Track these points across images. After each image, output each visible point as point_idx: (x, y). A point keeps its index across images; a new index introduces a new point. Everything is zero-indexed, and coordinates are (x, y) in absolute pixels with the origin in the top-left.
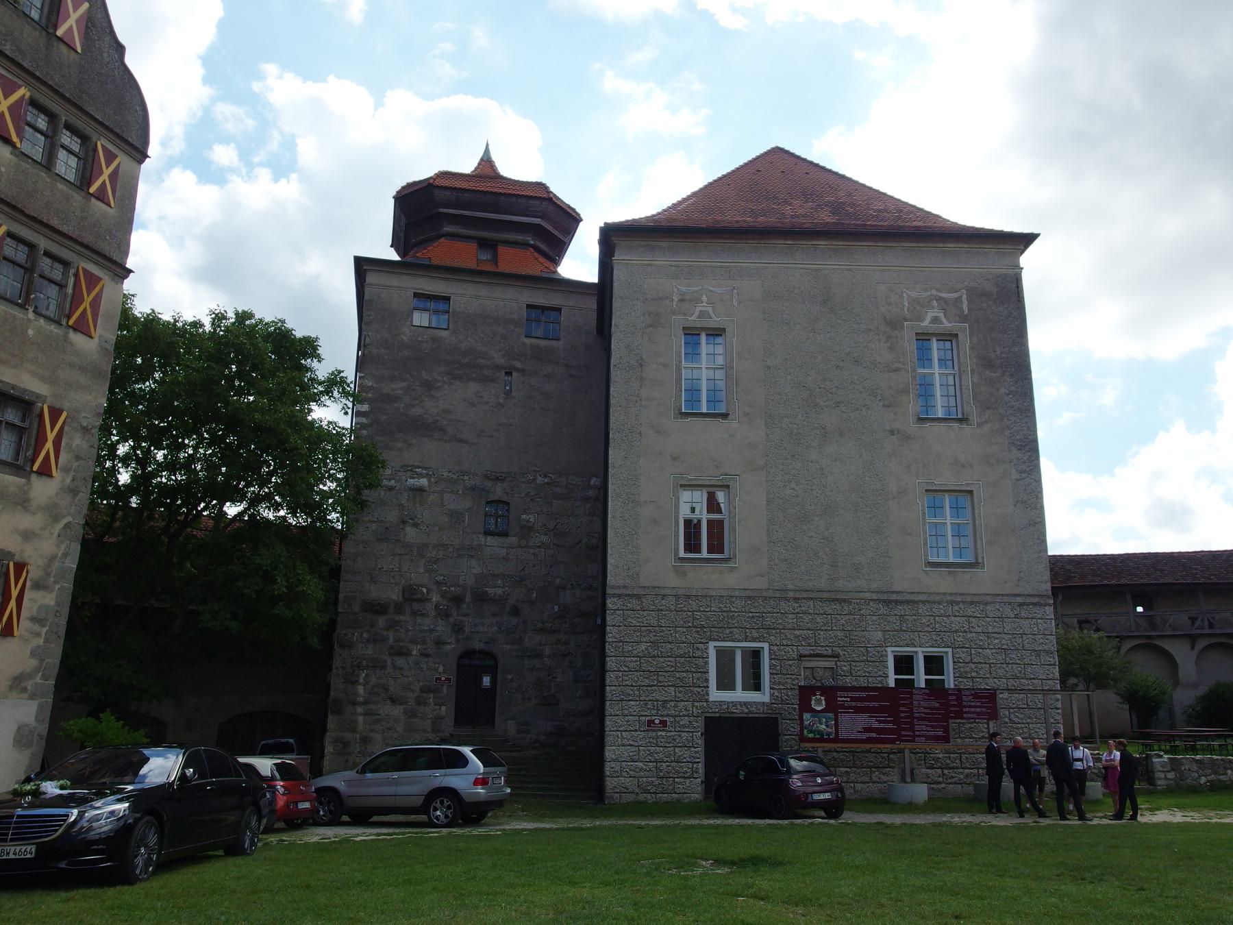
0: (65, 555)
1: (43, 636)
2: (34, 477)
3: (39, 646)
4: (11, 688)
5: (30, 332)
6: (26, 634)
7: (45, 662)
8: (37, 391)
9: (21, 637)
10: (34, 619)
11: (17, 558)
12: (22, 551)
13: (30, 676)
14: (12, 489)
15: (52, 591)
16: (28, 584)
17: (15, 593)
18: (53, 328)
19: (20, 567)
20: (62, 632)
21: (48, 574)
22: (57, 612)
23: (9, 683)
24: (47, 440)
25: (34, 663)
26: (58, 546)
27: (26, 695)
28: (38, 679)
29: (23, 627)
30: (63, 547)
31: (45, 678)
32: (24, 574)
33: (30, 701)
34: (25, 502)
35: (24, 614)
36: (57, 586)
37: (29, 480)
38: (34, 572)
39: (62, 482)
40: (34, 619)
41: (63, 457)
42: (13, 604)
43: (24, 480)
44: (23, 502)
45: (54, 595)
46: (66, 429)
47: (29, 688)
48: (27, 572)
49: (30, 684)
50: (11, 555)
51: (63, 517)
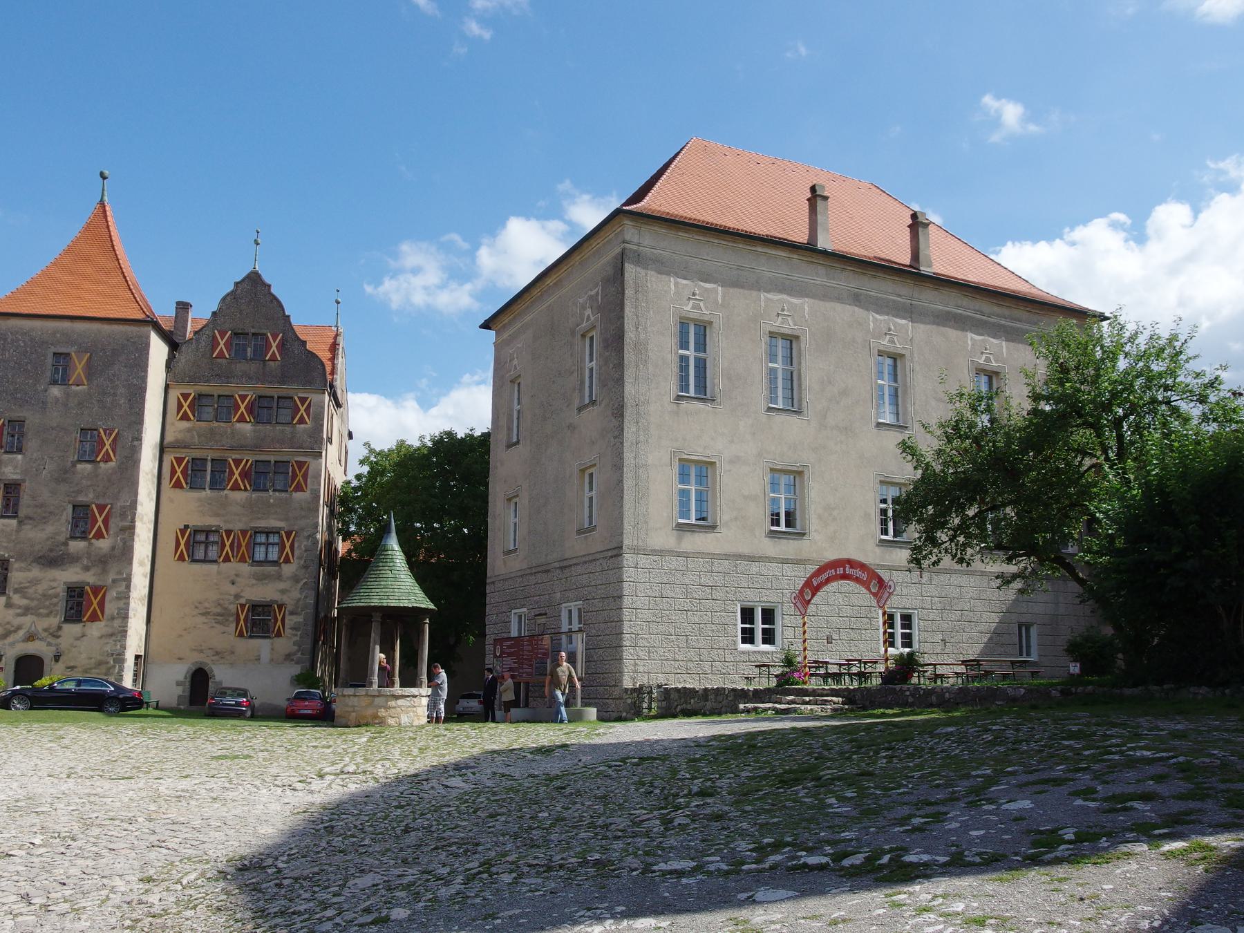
0: (306, 597)
2: (283, 565)
4: (285, 659)
5: (272, 501)
10: (291, 629)
11: (279, 603)
14: (273, 573)
16: (287, 612)
17: (279, 618)
18: (283, 495)
19: (280, 607)
25: (296, 648)
26: (301, 594)
28: (299, 655)
29: (288, 631)
30: (304, 594)
31: (302, 654)
35: (287, 626)
38: (289, 608)
41: (297, 553)
42: (279, 623)
43: (277, 568)
44: (279, 577)
45: (302, 616)
46: (296, 539)
50: (276, 602)
51: (302, 580)
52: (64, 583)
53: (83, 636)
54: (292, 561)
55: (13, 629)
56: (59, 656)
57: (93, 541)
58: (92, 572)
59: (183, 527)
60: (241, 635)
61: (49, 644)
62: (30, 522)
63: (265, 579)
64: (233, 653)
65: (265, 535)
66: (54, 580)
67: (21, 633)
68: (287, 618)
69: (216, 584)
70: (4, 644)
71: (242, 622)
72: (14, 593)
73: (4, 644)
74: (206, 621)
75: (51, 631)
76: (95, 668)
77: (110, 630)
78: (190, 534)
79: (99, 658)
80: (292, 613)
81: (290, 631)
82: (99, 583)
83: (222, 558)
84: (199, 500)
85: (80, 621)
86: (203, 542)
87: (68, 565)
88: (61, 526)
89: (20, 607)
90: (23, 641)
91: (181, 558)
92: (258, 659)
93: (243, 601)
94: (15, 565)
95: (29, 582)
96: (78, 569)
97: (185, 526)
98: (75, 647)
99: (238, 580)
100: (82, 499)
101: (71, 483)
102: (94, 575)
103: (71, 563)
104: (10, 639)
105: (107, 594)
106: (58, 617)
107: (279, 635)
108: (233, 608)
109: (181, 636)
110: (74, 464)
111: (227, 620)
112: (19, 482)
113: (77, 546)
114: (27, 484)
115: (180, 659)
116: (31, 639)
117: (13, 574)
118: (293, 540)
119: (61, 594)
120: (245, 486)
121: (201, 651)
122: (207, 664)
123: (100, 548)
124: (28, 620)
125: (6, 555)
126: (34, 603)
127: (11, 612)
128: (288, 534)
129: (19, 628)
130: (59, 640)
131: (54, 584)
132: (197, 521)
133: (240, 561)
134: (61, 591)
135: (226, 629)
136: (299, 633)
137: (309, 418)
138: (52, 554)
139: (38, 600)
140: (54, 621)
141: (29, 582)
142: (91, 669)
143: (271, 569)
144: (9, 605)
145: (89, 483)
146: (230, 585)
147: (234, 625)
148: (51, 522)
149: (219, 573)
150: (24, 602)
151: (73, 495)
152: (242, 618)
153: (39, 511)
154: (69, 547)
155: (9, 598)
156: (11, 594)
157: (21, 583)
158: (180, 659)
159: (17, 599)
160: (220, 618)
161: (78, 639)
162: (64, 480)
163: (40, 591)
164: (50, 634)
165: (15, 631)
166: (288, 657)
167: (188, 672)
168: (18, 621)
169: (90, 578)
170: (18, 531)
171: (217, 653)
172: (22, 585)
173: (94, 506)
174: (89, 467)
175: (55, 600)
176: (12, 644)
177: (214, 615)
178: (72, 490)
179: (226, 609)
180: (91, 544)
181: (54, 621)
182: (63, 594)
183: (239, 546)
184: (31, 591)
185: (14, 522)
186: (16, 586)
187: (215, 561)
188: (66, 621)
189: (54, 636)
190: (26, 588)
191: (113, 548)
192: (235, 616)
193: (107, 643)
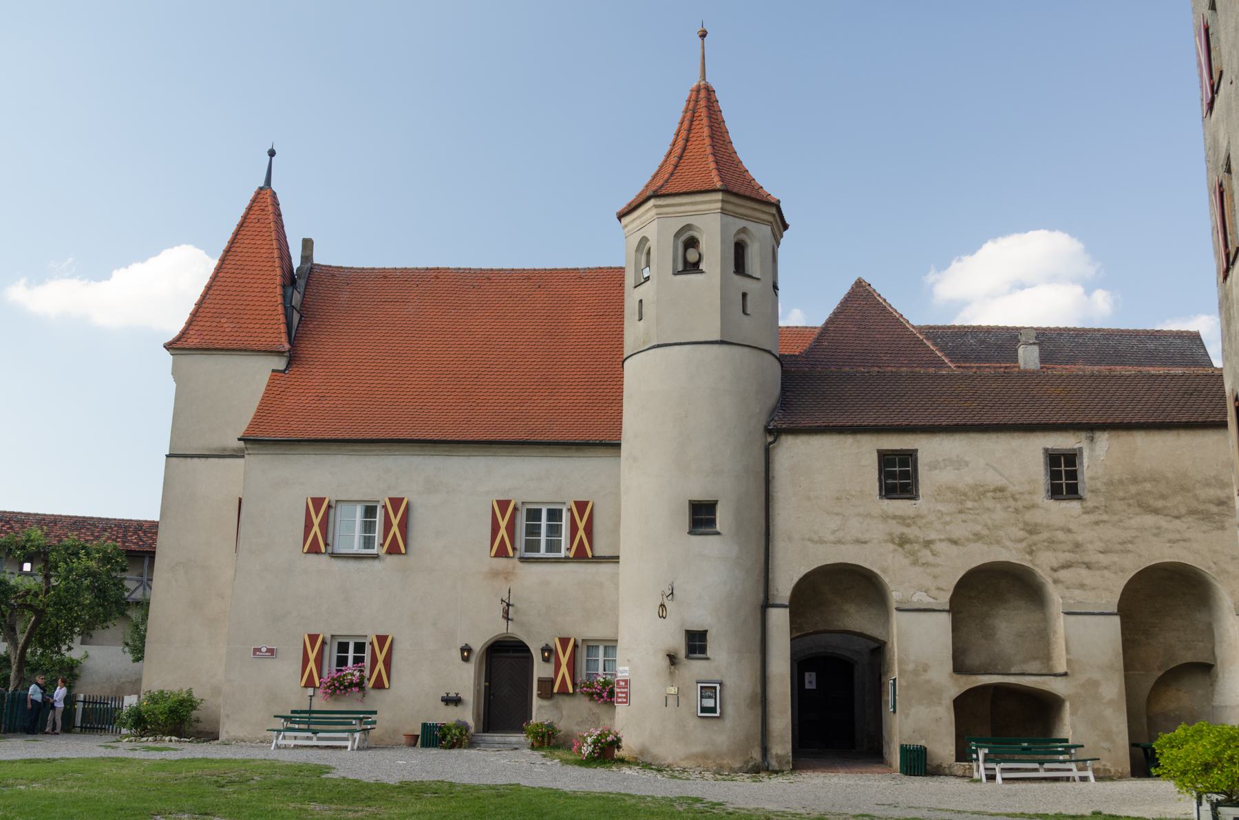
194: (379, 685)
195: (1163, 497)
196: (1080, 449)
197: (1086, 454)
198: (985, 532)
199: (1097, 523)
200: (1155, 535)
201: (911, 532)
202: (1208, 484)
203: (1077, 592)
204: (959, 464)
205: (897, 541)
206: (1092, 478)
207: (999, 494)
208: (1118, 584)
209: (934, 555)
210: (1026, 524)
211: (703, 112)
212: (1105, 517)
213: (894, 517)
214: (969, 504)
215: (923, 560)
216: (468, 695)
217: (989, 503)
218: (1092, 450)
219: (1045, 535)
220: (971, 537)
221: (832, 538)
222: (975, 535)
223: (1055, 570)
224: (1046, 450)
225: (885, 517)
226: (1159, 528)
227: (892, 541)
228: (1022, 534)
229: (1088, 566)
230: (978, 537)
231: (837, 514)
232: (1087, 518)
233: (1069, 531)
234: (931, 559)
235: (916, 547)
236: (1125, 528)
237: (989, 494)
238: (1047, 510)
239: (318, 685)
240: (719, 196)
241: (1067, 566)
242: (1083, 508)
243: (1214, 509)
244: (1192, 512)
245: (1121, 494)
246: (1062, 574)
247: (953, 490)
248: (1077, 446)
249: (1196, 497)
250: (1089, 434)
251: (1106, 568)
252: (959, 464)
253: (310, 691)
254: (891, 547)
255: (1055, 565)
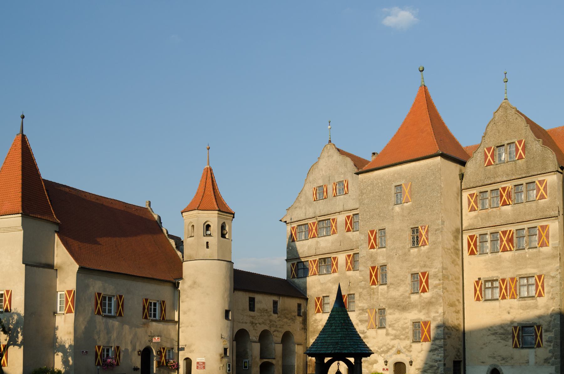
0: (555, 319)
1: (552, 346)
3: (551, 349)
4: (544, 362)
6: (546, 346)
7: (555, 354)
8: (533, 272)
9: (545, 347)
10: (547, 341)
11: (538, 324)
12: (539, 322)
13: (550, 358)
15: (552, 331)
16: (543, 331)
17: (539, 335)
19: (539, 327)
20: (559, 344)
21: (550, 327)
22: (555, 338)
23: (544, 361)
24: (539, 286)
27: (550, 364)
28: (553, 359)
31: (555, 359)
32: (541, 328)
33: (552, 366)
34: (537, 307)
35: (544, 340)
36: (554, 330)
37: (537, 300)
38: (544, 327)
39: (548, 297)
40: (547, 341)
42: (539, 338)
45: (553, 333)
47: (551, 362)
48: (542, 328)
49: (551, 361)
50: (535, 324)
52: (411, 320)
53: (422, 351)
54: (543, 295)
55: (390, 347)
56: (412, 362)
57: (422, 294)
58: (422, 314)
59: (477, 280)
60: (516, 347)
61: (407, 356)
62: (393, 286)
63: (528, 309)
64: (512, 358)
65: (526, 279)
66: (406, 319)
67: (394, 349)
68: (543, 334)
69: (499, 315)
70: (387, 356)
71: (516, 338)
72: (389, 327)
73: (387, 356)
74: (495, 338)
75: (407, 348)
76: (429, 369)
77: (436, 347)
78: (482, 284)
79: (431, 363)
80: (546, 331)
81: (546, 343)
82: (427, 319)
83: (501, 297)
84: (485, 261)
85: (420, 342)
86: (490, 288)
87: (411, 310)
88: (405, 288)
89: (392, 335)
90: (395, 354)
91: (478, 299)
92: (528, 362)
93: (516, 325)
94: (388, 311)
95: (395, 321)
96: (416, 312)
97: (478, 278)
98: (419, 357)
99: (512, 310)
100: (415, 270)
101: (409, 261)
102: (424, 314)
103: (413, 308)
104: (389, 354)
105: (431, 325)
106: (410, 340)
107: (539, 346)
108: (510, 329)
109: (482, 348)
110: (409, 251)
111: (507, 337)
112: (385, 264)
113: (415, 298)
114: (389, 265)
115: (483, 363)
116: (398, 353)
117: (387, 316)
118: (543, 281)
119: (410, 327)
120: (510, 248)
121: (494, 358)
122: (498, 366)
123: (426, 298)
124: (396, 342)
125: (384, 306)
126: (399, 332)
127: (389, 337)
128: (540, 277)
129: (393, 347)
130: (412, 353)
131: (406, 321)
132: (486, 275)
133: (511, 298)
134: (410, 325)
135: (507, 343)
136: (552, 344)
137: (547, 195)
138: (404, 304)
139: (400, 331)
140: (408, 342)
141: (395, 321)
142: (427, 370)
143: (530, 302)
144: (387, 334)
145: (417, 260)
146: (508, 314)
147: (511, 340)
148: (402, 285)
149: (500, 307)
150: (394, 332)
151: (410, 268)
152: (516, 335)
153: (396, 279)
154: (412, 299)
155: (387, 330)
156: (388, 328)
157: (392, 321)
158: (483, 363)
159: (391, 331)
160: (503, 336)
161: (419, 352)
162: (405, 260)
163: (400, 326)
164: (407, 350)
165: (391, 349)
166: (546, 361)
167: (488, 371)
168: (392, 343)
169: (421, 316)
170: (388, 292)
171: (503, 359)
172: (392, 323)
173: (420, 274)
174: (415, 250)
175: (407, 330)
176: (391, 356)
177: (500, 334)
178: (409, 265)
179: (506, 330)
180: (421, 296)
181: (408, 342)
182: (411, 327)
183: (511, 288)
184: (396, 325)
185: (385, 287)
186: (390, 323)
187: (497, 299)
188: (413, 342)
189: (408, 351)
190: (394, 324)
191: (432, 297)
192: (512, 335)
193: (434, 355)
194: (118, 364)
195: (288, 315)
196: (278, 301)
197: (278, 302)
198: (264, 321)
199: (279, 320)
200: (287, 324)
201: (254, 321)
202: (293, 312)
203: (276, 338)
204: (260, 302)
205: (251, 323)
206: (279, 309)
207: (266, 312)
208: (281, 335)
209: (257, 327)
210: (270, 320)
211: (209, 181)
212: (280, 319)
213: (251, 316)
214: (262, 314)
215: (255, 329)
216: (139, 367)
217: (265, 314)
218: (279, 301)
219: (272, 323)
220: (262, 323)
221: (241, 321)
222: (263, 322)
223: (273, 332)
224: (273, 300)
225: (250, 316)
226: (287, 322)
227: (250, 323)
228: (269, 322)
229: (278, 331)
230: (263, 323)
231: (243, 315)
232: (278, 319)
233: (275, 322)
234: (256, 328)
235: (254, 325)
236: (283, 322)
237: (265, 311)
238: (273, 316)
239: (101, 365)
240: (217, 212)
241: (275, 331)
242: (278, 316)
243: (294, 318)
244: (292, 319)
245: (283, 313)
246: (275, 333)
247: (260, 309)
248: (277, 300)
249: (292, 315)
250: (278, 297)
251: (280, 332)
252: (260, 302)
253: (99, 367)
254: (250, 324)
255: (273, 331)
